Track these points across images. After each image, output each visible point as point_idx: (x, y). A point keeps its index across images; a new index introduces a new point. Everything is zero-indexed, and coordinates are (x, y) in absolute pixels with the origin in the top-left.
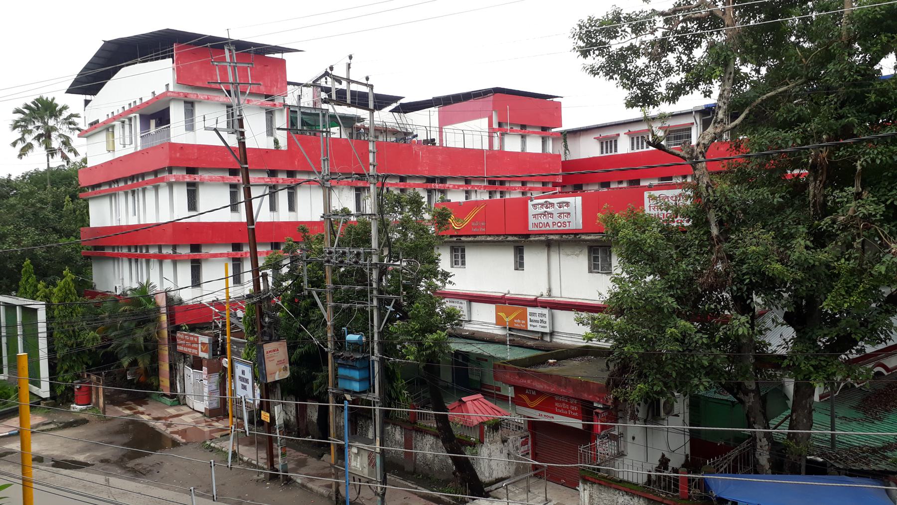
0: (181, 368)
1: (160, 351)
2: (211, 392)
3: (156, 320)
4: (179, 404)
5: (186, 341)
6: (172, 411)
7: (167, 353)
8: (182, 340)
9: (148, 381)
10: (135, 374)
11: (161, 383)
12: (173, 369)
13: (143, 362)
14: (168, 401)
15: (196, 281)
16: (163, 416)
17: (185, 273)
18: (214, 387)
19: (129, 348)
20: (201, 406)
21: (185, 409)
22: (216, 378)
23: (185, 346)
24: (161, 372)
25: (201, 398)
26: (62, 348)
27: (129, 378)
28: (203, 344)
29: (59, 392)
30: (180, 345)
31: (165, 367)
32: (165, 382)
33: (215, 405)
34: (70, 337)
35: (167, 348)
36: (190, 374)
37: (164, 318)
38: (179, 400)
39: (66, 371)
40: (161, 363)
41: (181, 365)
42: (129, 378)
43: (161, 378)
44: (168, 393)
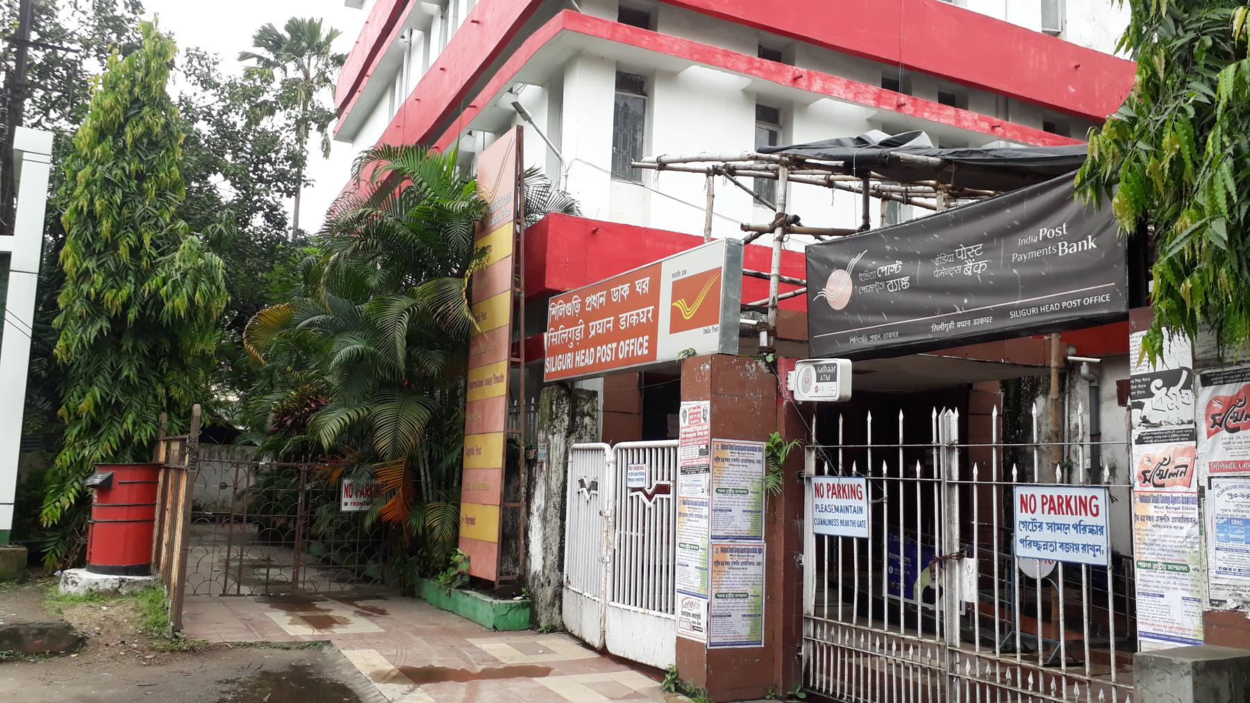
0: (556, 455)
1: (474, 395)
2: (723, 550)
3: (472, 249)
4: (533, 624)
5: (588, 316)
6: (503, 649)
7: (501, 389)
8: (570, 321)
9: (415, 523)
10: (371, 493)
11: (465, 531)
12: (519, 463)
13: (398, 424)
14: (485, 606)
15: (628, 156)
16: (455, 663)
17: (591, 101)
18: (742, 517)
19: (354, 364)
20: (651, 637)
21: (558, 649)
22: (748, 466)
23: (587, 343)
24: (469, 480)
25: (649, 582)
26: (84, 321)
27: (348, 504)
28: (684, 288)
29: (50, 513)
30: (562, 348)
31: (486, 455)
32: (482, 522)
33: (741, 628)
34: (117, 276)
35: (502, 368)
36: (597, 475)
37: (502, 242)
38: (531, 605)
39: (93, 429)
40: (472, 441)
41: (558, 440)
42: (348, 504)
43: (466, 510)
44: (486, 568)
